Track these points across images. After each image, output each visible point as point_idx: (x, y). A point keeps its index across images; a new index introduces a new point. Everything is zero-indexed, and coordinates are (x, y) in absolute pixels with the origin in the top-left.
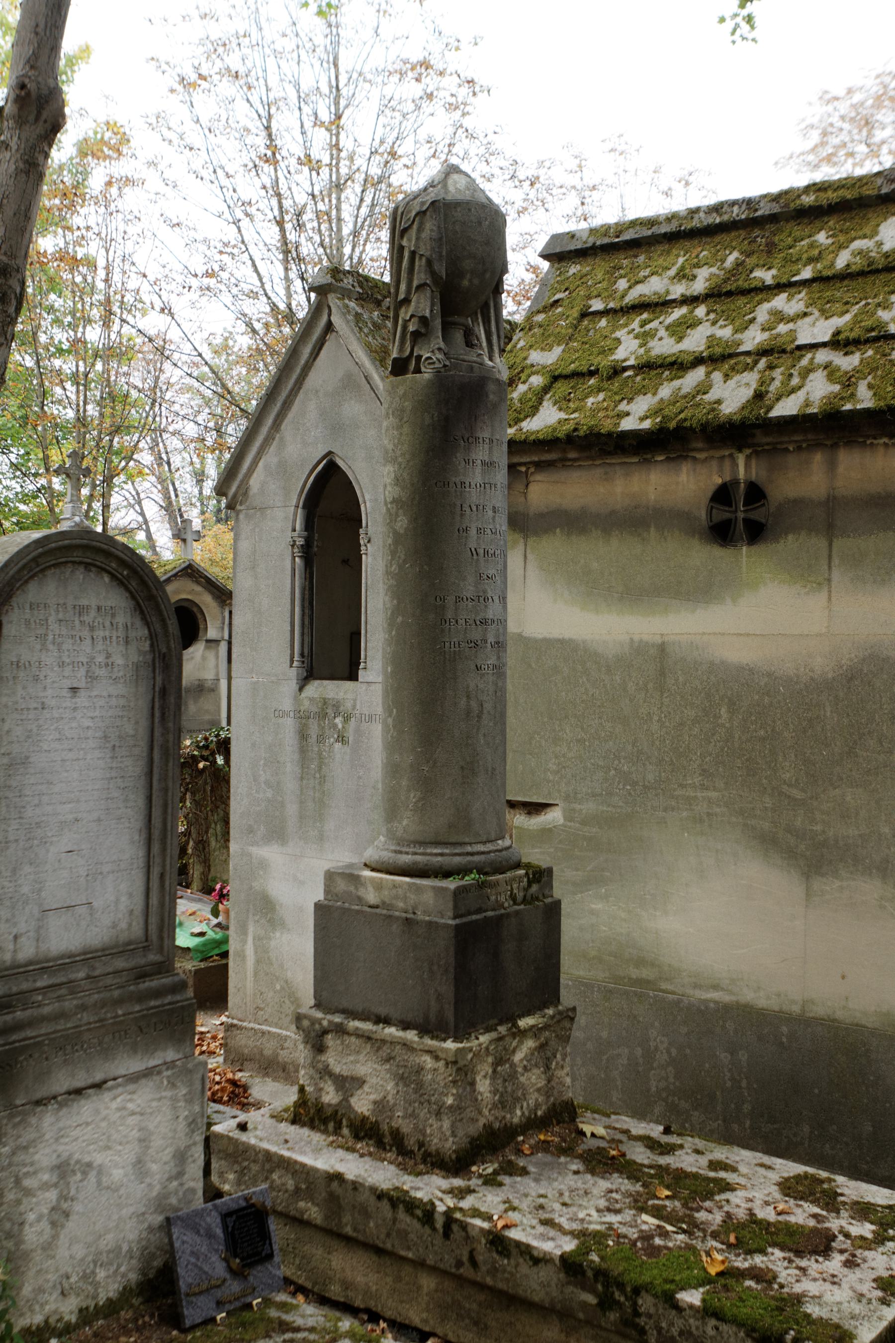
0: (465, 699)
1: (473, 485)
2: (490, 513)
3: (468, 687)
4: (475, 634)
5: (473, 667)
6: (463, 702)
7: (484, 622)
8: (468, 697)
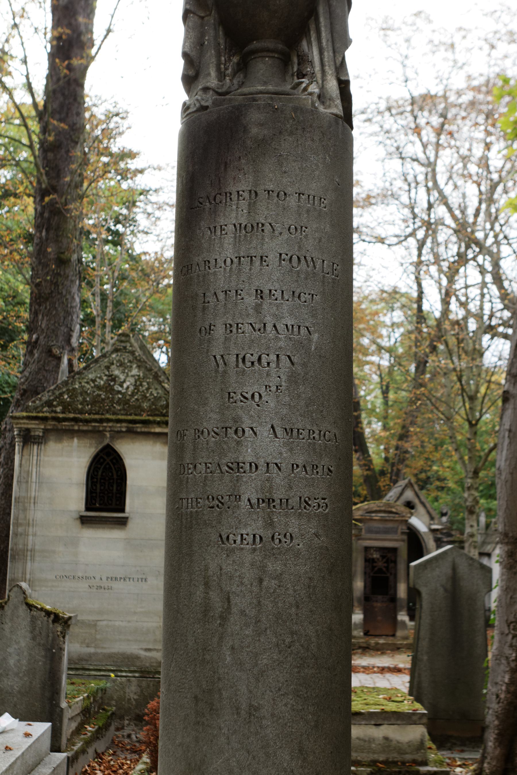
0: (202, 588)
1: (220, 263)
2: (251, 300)
3: (207, 568)
4: (220, 487)
5: (214, 537)
6: (199, 593)
7: (237, 467)
8: (207, 585)
